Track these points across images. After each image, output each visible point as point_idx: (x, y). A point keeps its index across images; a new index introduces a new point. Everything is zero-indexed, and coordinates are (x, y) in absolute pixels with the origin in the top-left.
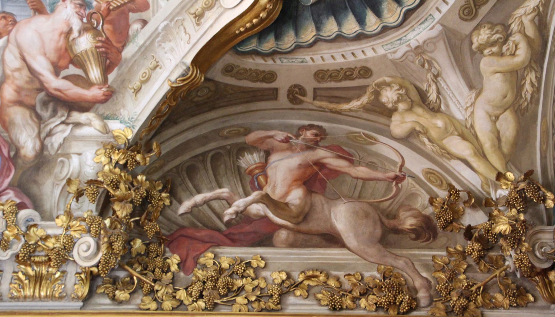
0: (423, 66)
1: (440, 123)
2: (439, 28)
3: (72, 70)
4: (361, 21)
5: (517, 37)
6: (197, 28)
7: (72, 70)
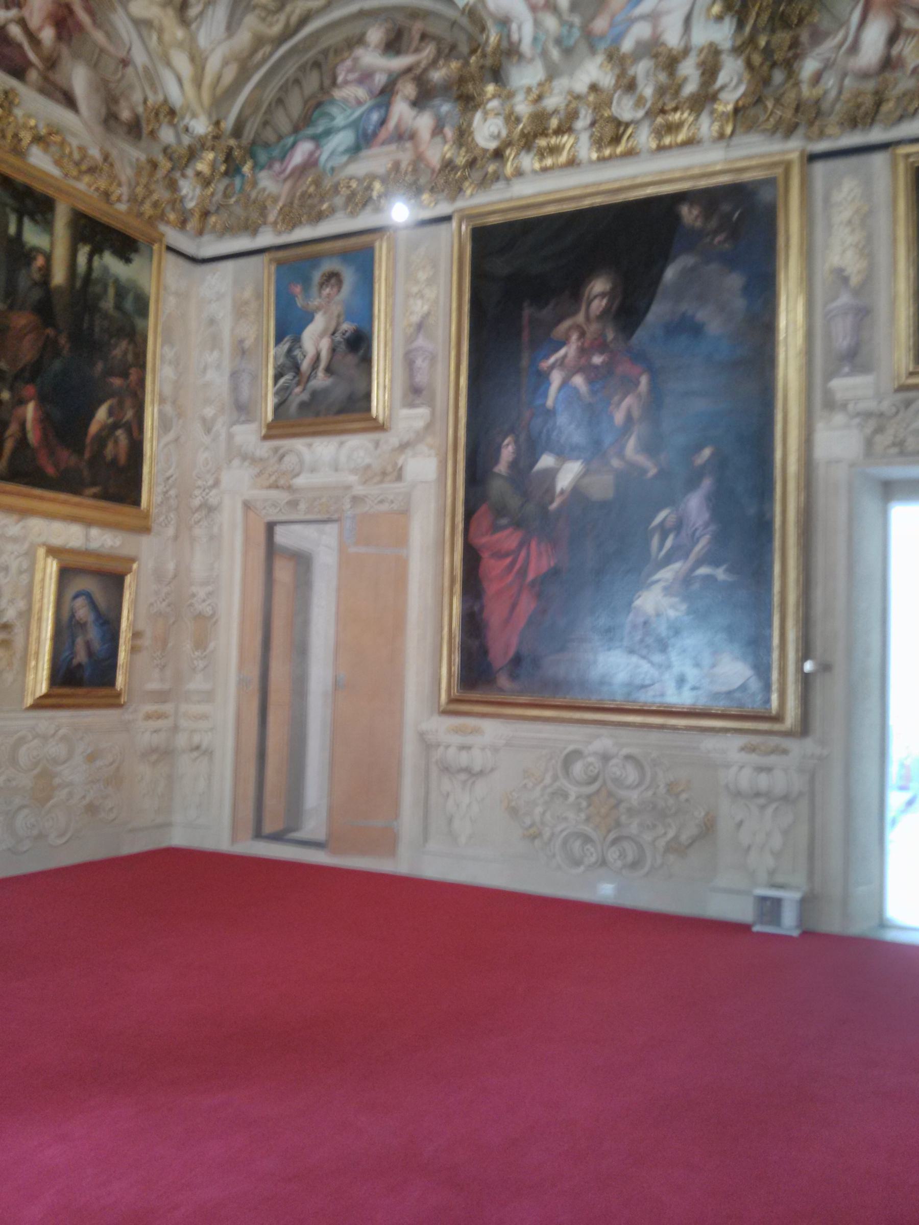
1: (180, 34)
5: (282, 18)
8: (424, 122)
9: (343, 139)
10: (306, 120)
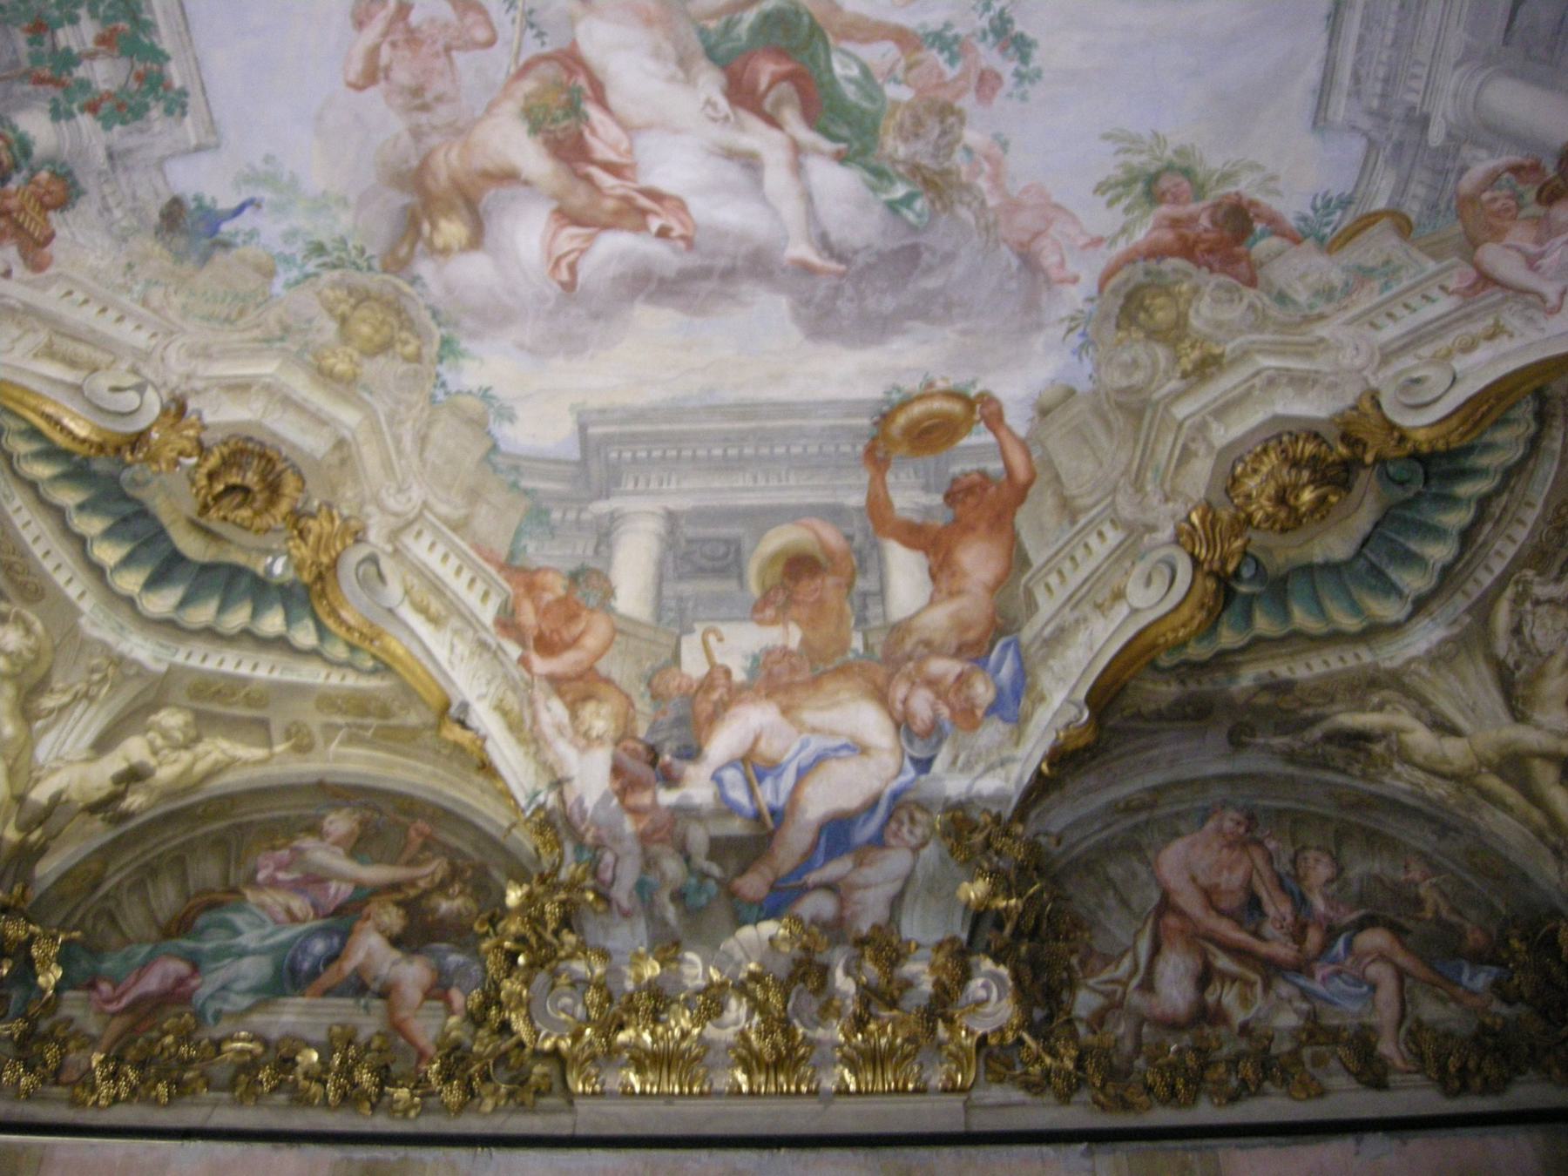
0: (93, 671)
2: (163, 668)
4: (127, 562)
5: (186, 757)
6: (30, 355)
8: (412, 974)
9: (254, 969)
10: (182, 926)
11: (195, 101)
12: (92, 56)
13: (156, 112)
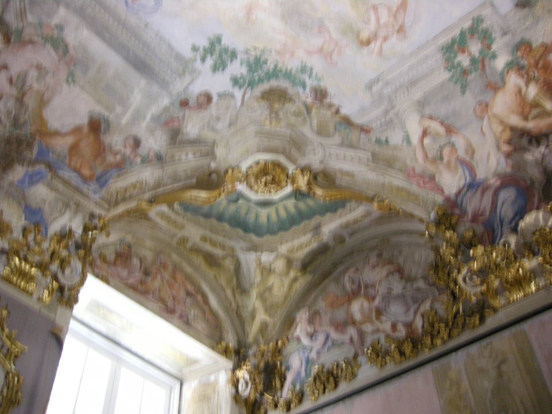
3: (534, 112)
7: (534, 112)
11: (475, 15)
12: (470, 54)
13: (484, 25)
